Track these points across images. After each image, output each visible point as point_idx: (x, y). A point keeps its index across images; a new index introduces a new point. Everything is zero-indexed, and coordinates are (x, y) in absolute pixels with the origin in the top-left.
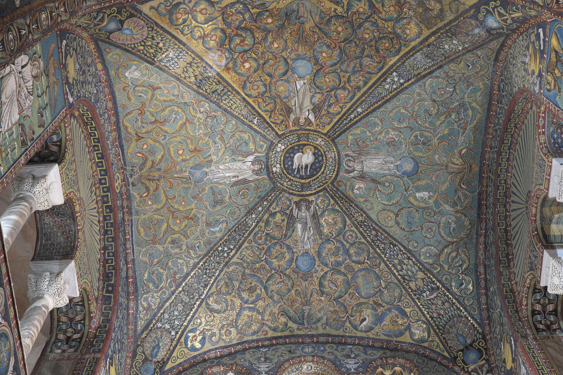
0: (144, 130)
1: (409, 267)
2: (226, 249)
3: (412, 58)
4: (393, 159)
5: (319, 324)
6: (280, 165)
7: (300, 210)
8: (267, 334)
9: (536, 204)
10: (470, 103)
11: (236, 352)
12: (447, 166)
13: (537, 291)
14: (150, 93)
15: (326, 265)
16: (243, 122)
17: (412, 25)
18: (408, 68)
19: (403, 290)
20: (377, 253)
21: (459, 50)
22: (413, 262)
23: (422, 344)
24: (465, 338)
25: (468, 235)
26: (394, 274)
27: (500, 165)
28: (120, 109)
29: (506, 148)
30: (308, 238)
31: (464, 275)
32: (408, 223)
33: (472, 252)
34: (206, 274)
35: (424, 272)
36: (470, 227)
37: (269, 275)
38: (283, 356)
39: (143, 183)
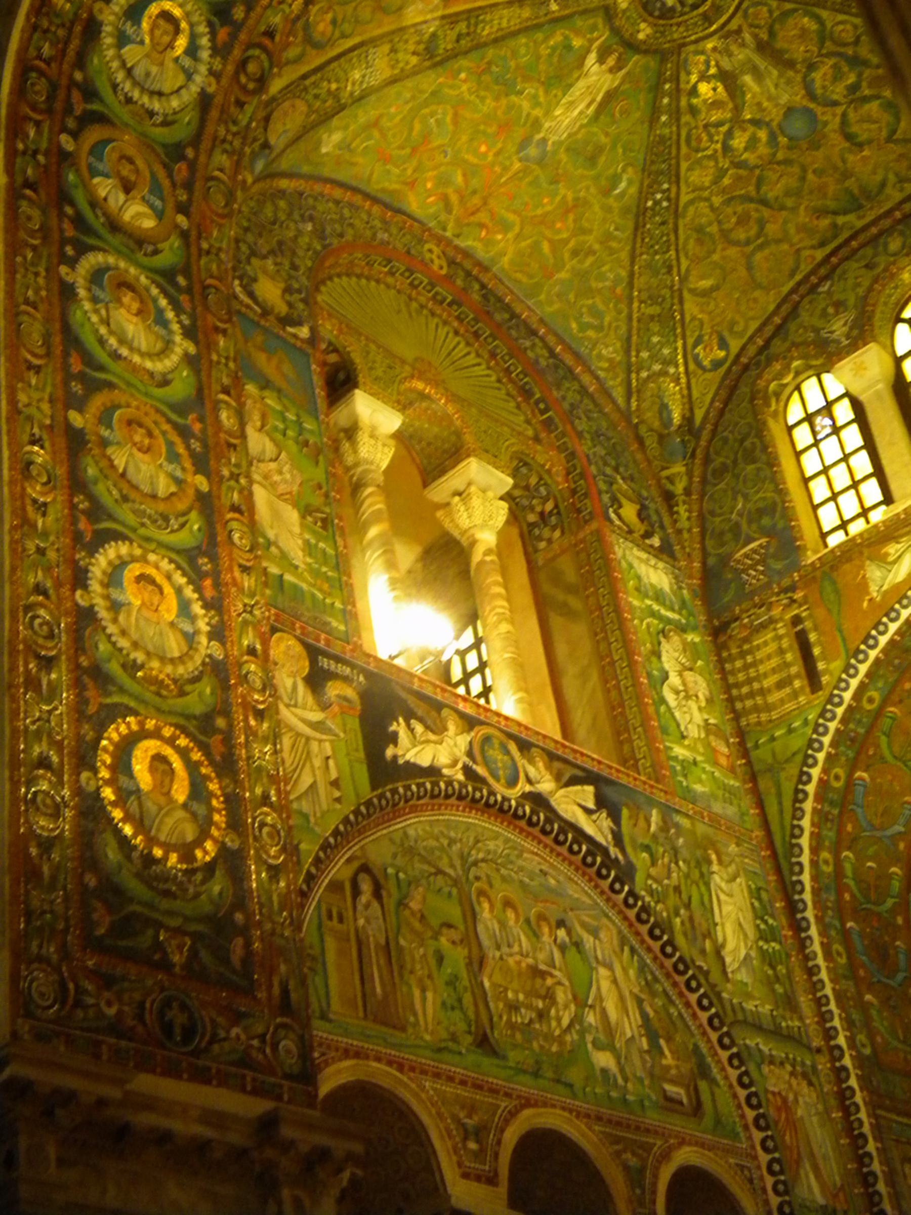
0: (409, 172)
2: (659, 196)
5: (888, 190)
6: (645, 21)
7: (730, 55)
8: (813, 258)
11: (785, 320)
14: (376, 134)
15: (835, 104)
16: (538, 27)
28: (354, 183)
30: (776, 86)
34: (656, 253)
37: (754, 181)
38: (858, 285)
39: (468, 225)
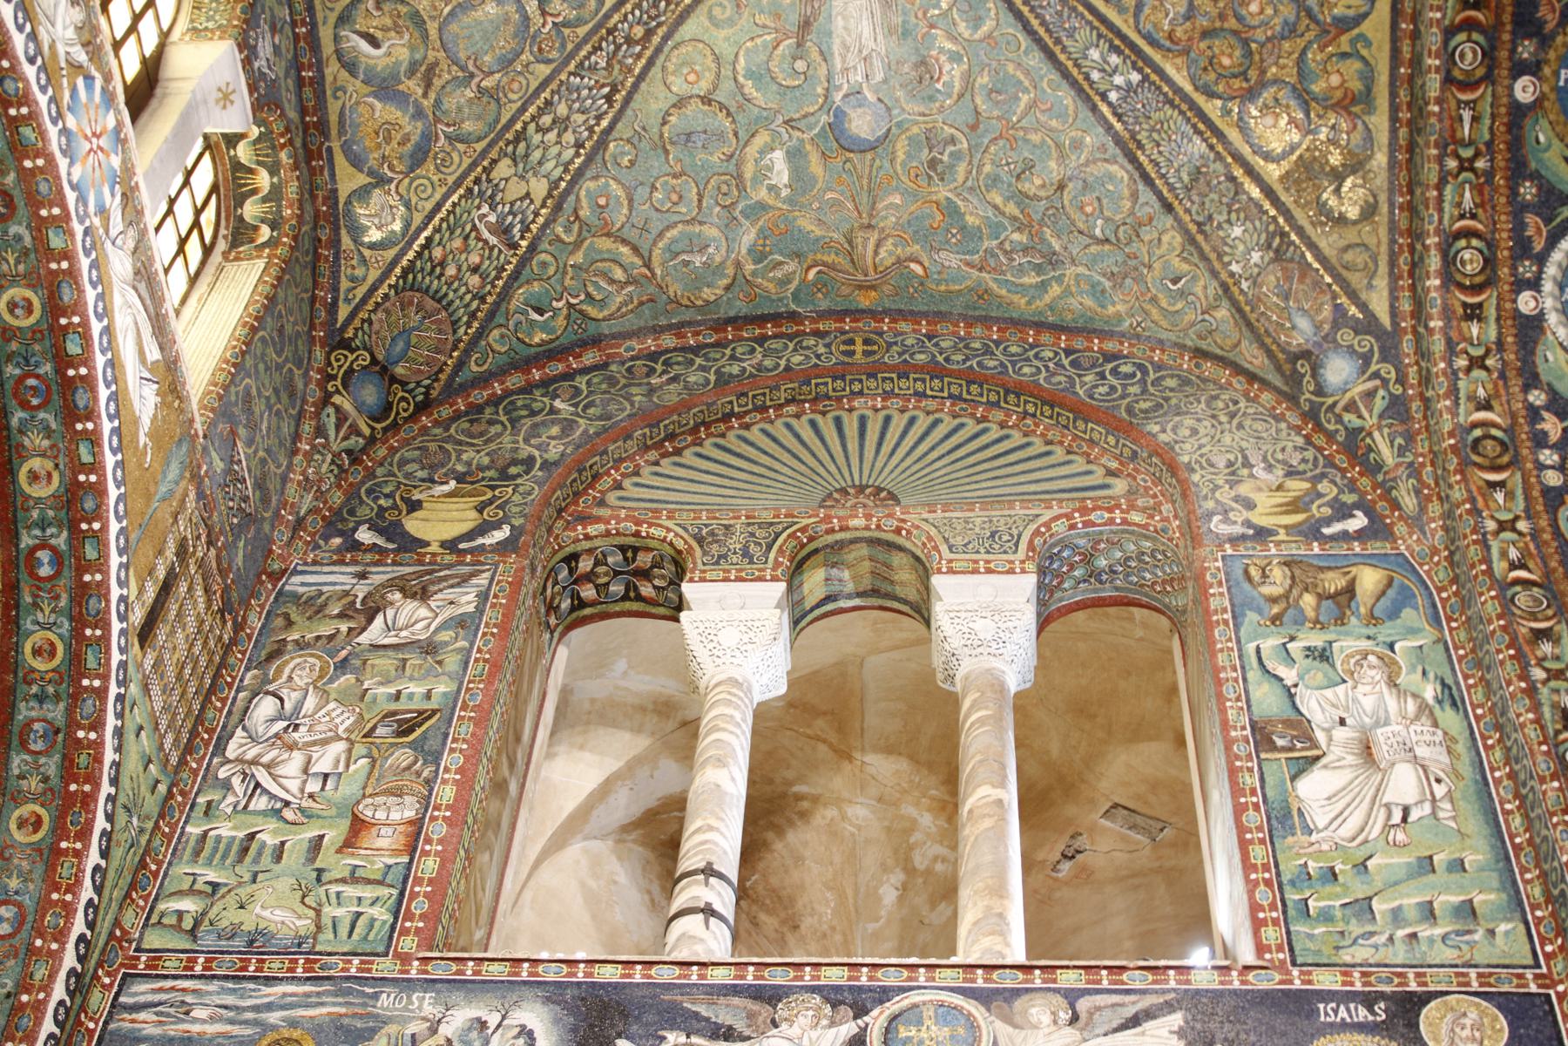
1: (554, 150)
3: (1189, 130)
4: (879, 77)
9: (878, 526)
10: (1059, 280)
12: (870, 226)
13: (630, 554)
17: (1295, 136)
18: (1156, 116)
19: (483, 144)
20: (578, 47)
21: (1230, 263)
22: (571, 161)
23: (343, 232)
24: (403, 356)
25: (678, 303)
26: (523, 109)
27: (903, 375)
29: (955, 390)
31: (565, 311)
32: (689, 135)
33: (632, 322)
35: (550, 195)
36: (699, 303)
